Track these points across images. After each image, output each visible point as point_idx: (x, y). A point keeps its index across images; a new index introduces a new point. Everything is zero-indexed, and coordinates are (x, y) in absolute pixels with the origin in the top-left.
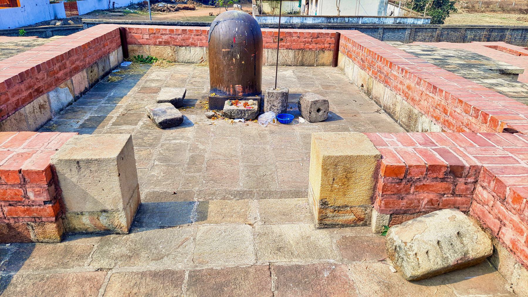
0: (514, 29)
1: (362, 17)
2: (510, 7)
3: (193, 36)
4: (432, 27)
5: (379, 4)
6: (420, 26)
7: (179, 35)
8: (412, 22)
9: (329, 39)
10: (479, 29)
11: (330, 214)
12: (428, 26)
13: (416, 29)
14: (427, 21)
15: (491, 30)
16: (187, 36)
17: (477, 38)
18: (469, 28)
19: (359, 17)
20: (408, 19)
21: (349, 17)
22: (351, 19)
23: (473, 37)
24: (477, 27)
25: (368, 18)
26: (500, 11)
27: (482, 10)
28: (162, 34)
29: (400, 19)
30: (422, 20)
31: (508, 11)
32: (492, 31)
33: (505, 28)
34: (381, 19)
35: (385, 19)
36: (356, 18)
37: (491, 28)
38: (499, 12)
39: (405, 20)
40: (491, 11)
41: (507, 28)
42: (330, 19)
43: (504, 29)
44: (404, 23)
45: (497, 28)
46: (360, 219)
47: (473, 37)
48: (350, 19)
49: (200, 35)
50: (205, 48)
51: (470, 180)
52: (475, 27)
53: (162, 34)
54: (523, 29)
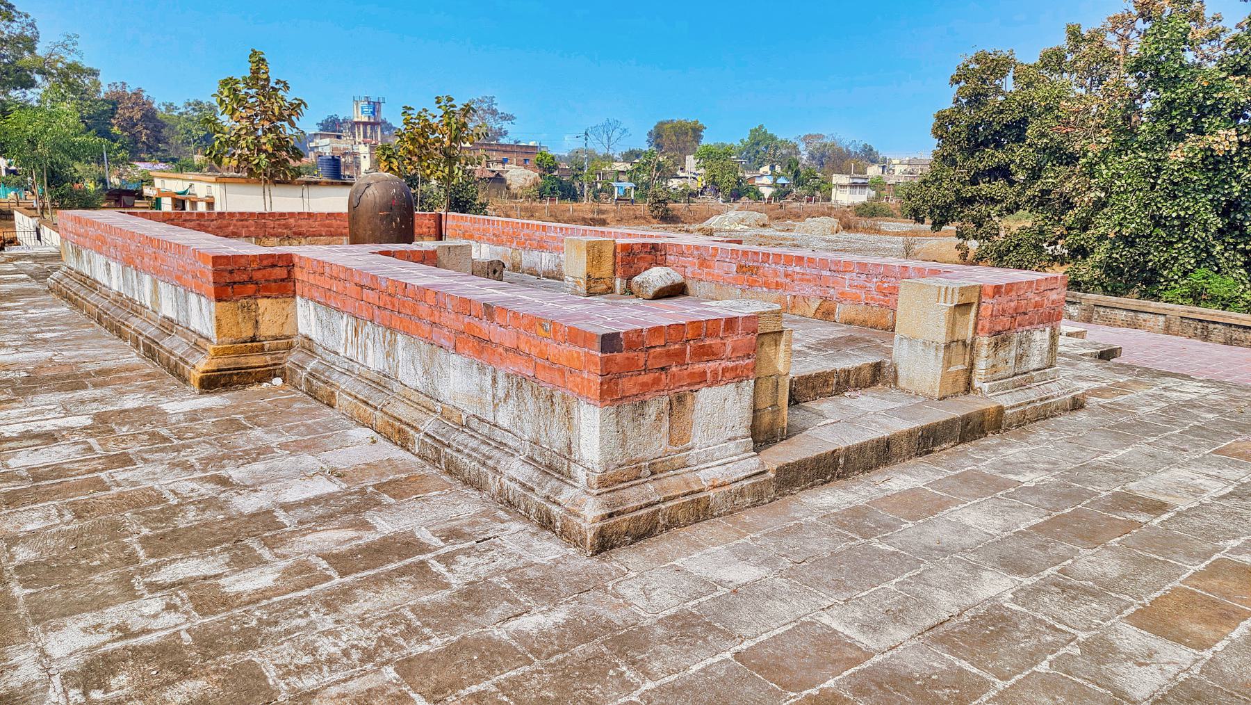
2: (567, 214)
3: (235, 222)
7: (213, 220)
9: (427, 221)
11: (593, 285)
16: (225, 222)
28: (185, 220)
46: (609, 288)
49: (246, 220)
50: (254, 239)
51: (663, 253)
53: (185, 220)
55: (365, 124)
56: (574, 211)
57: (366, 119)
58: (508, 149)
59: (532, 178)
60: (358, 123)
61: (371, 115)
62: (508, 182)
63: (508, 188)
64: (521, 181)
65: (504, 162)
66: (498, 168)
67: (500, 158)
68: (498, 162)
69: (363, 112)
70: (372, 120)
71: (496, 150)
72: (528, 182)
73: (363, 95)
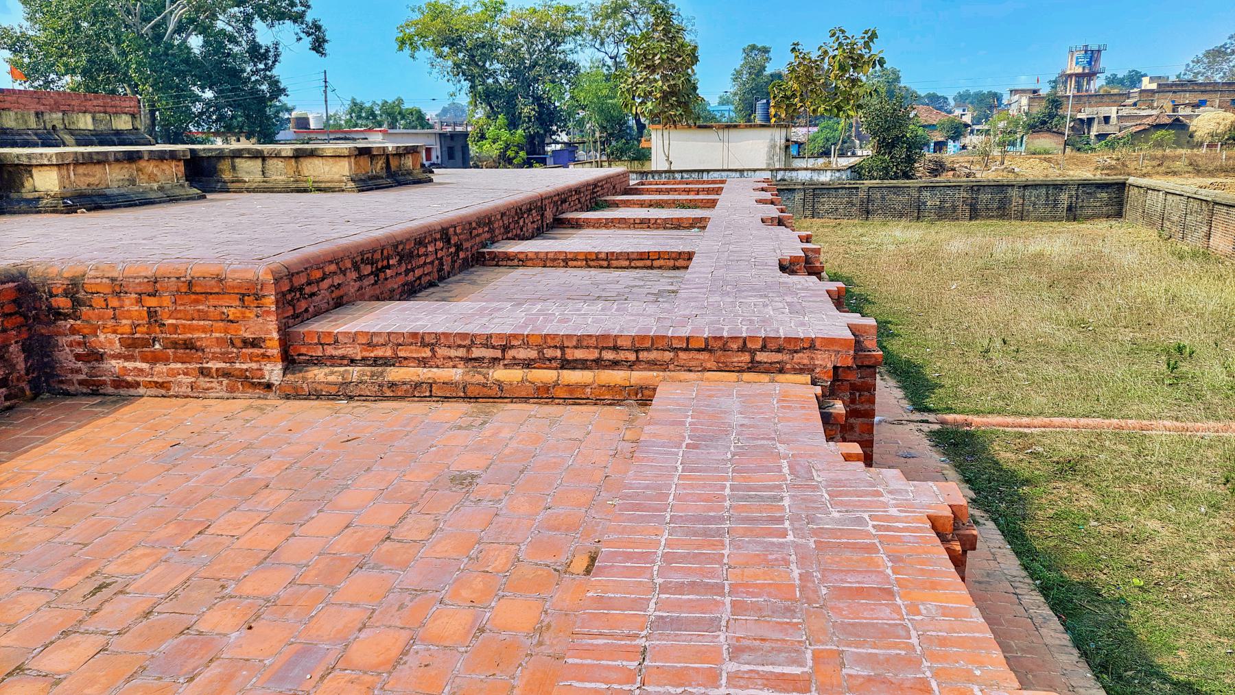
0: (1025, 187)
1: (708, 171)
4: (847, 186)
5: (766, 149)
6: (822, 185)
8: (807, 178)
10: (949, 187)
12: (839, 184)
13: (814, 189)
14: (837, 174)
15: (975, 188)
17: (946, 205)
18: (927, 187)
19: (703, 171)
20: (799, 172)
21: (682, 172)
22: (685, 175)
23: (938, 203)
24: (943, 184)
25: (718, 173)
26: (1189, 172)
27: (1145, 171)
29: (782, 172)
30: (829, 173)
31: (1209, 172)
32: (979, 190)
33: (1006, 183)
34: (745, 173)
35: (753, 173)
36: (697, 174)
37: (975, 184)
38: (1187, 175)
39: (794, 174)
40: (1167, 173)
41: (1010, 183)
42: (647, 176)
43: (1003, 185)
44: (792, 180)
45: (986, 184)
47: (938, 203)
48: (684, 174)
52: (937, 185)
54: (1048, 186)
55: (1077, 75)
56: (1228, 158)
57: (1079, 70)
58: (1208, 88)
59: (1228, 122)
60: (1070, 76)
61: (1087, 66)
62: (1192, 129)
63: (1191, 136)
64: (1212, 127)
65: (1196, 106)
66: (1188, 111)
67: (1196, 101)
68: (1186, 105)
69: (1077, 63)
70: (1087, 71)
71: (1190, 91)
72: (1221, 127)
73: (1081, 45)
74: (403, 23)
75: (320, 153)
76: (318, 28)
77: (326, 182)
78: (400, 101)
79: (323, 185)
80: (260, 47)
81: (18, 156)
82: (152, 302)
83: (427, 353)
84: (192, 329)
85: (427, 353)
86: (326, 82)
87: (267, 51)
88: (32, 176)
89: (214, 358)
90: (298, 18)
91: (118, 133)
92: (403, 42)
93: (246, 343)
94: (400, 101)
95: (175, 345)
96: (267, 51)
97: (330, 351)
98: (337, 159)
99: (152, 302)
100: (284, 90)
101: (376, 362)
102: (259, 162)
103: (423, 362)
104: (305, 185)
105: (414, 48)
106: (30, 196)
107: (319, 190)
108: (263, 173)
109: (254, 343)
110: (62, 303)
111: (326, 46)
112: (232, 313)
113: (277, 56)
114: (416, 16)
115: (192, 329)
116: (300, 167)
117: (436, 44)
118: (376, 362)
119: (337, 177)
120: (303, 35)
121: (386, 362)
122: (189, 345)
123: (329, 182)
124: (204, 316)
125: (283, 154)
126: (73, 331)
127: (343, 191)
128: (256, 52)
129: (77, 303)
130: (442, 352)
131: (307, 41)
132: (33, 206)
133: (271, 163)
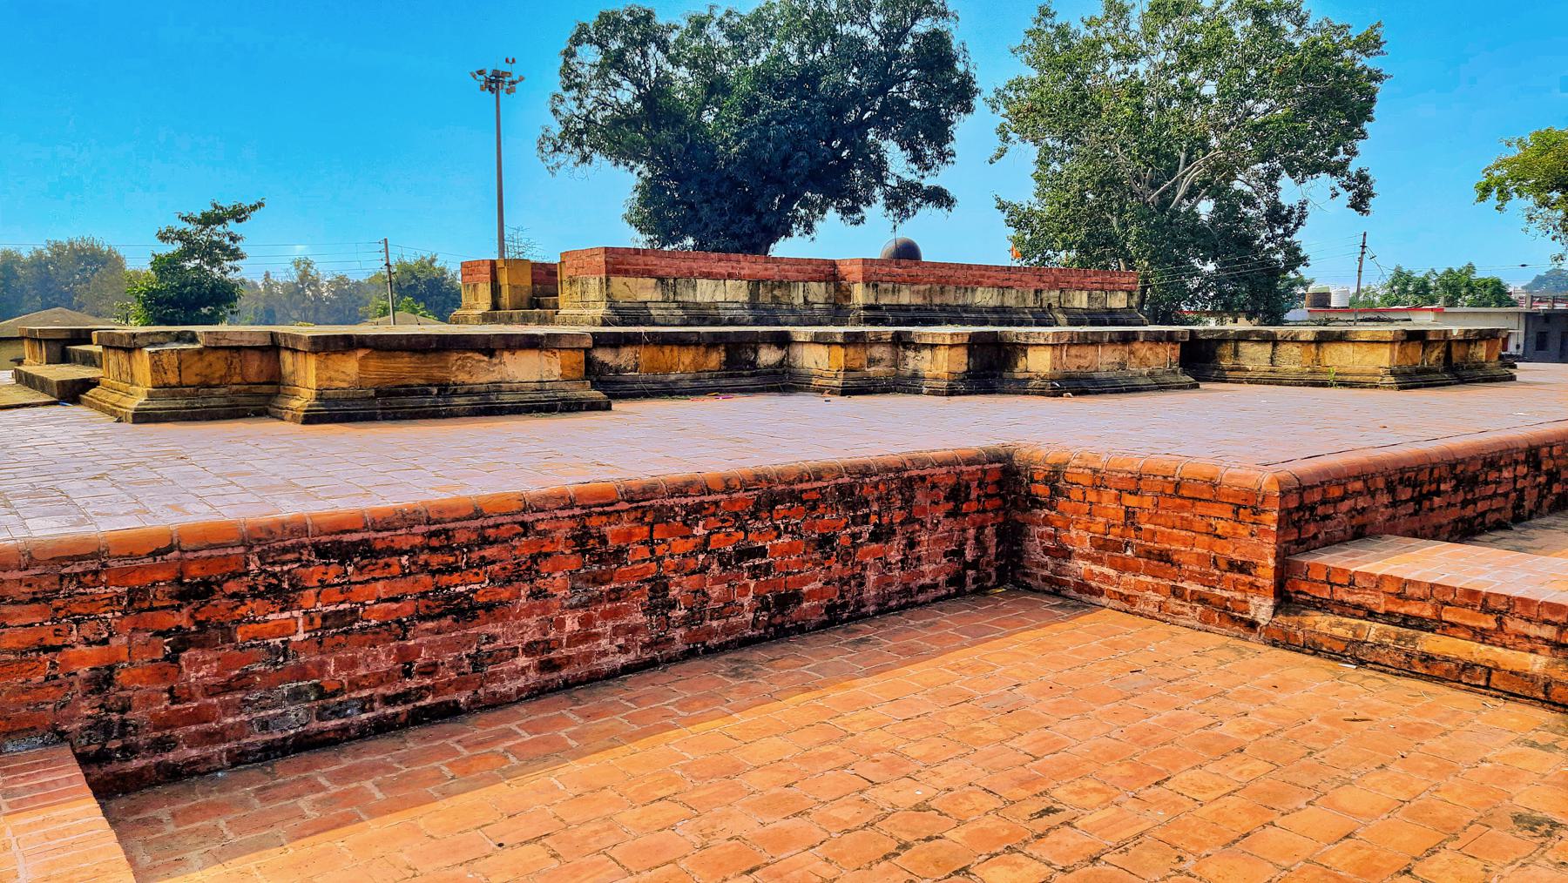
74: (1492, 164)
75: (1352, 337)
76: (1363, 178)
77: (1353, 375)
78: (1470, 268)
79: (1349, 378)
80: (1283, 208)
81: (1017, 335)
82: (1130, 501)
83: (1490, 623)
84: (1170, 539)
85: (1490, 623)
86: (1363, 247)
87: (1291, 212)
88: (1026, 356)
89: (1191, 577)
90: (1337, 170)
91: (1111, 311)
92: (1486, 190)
93: (1233, 566)
94: (1470, 268)
95: (1149, 554)
96: (1291, 212)
97: (1341, 594)
98: (1375, 345)
99: (1130, 501)
100: (1305, 258)
101: (1406, 621)
102: (1269, 347)
103: (1481, 635)
104: (1324, 377)
105: (1504, 195)
106: (1021, 376)
107: (1343, 384)
108: (1272, 360)
109: (1243, 568)
110: (1041, 490)
111: (1371, 201)
112: (1222, 527)
113: (1302, 217)
114: (1515, 152)
115: (1170, 539)
116: (1321, 354)
117: (1539, 188)
118: (1406, 621)
119: (1370, 369)
120: (1341, 190)
121: (1422, 624)
122: (1165, 557)
123: (1358, 375)
124: (1187, 526)
125: (1302, 338)
126: (1047, 522)
127: (1377, 387)
128: (1277, 215)
129: (1056, 491)
130: (1513, 625)
131: (1346, 196)
132: (1022, 388)
133: (1283, 348)
